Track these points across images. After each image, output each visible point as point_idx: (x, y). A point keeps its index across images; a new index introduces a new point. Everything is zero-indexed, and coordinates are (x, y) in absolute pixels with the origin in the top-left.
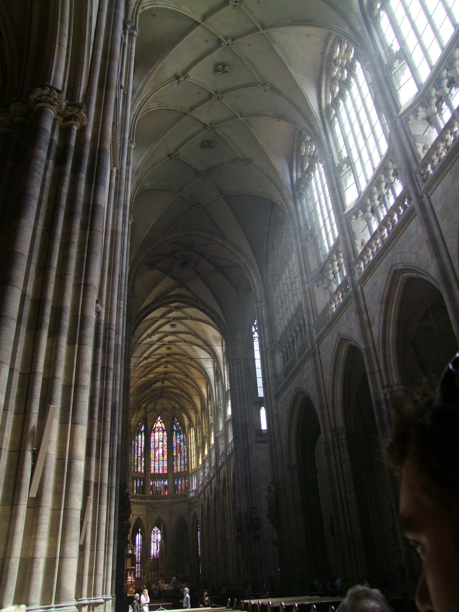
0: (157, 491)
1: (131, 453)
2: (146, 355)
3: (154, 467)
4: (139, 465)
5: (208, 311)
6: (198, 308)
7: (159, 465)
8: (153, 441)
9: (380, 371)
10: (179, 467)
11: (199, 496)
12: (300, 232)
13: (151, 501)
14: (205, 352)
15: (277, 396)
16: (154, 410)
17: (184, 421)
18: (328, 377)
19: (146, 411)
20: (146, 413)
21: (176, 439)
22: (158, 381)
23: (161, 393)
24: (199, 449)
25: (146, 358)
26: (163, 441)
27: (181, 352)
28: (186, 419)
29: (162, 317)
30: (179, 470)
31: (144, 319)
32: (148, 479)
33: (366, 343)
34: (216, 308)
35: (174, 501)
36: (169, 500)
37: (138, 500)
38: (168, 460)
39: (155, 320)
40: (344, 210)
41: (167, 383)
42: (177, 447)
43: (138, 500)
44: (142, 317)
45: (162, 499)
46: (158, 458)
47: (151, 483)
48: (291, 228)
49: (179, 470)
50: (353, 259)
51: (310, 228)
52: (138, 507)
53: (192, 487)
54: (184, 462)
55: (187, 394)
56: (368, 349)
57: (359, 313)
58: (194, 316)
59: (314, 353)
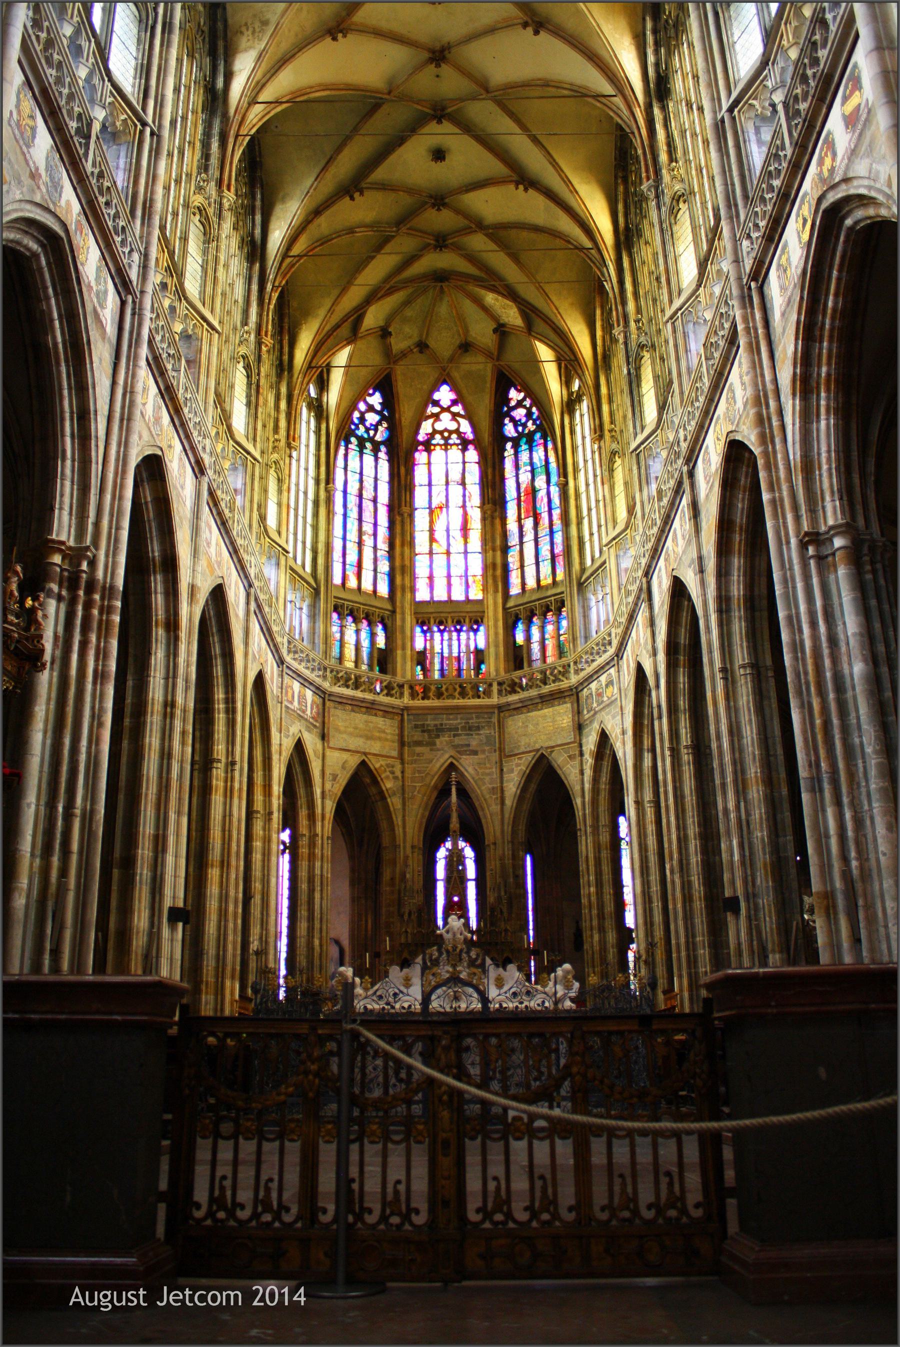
0: (442, 670)
1: (330, 513)
3: (431, 578)
4: (368, 564)
7: (450, 566)
10: (530, 572)
13: (419, 703)
16: (422, 346)
21: (517, 467)
24: (611, 461)
26: (463, 483)
30: (531, 583)
32: (403, 620)
35: (513, 698)
36: (495, 700)
37: (359, 694)
38: (484, 551)
42: (519, 498)
43: (359, 694)
45: (463, 694)
47: (419, 644)
49: (531, 583)
52: (360, 719)
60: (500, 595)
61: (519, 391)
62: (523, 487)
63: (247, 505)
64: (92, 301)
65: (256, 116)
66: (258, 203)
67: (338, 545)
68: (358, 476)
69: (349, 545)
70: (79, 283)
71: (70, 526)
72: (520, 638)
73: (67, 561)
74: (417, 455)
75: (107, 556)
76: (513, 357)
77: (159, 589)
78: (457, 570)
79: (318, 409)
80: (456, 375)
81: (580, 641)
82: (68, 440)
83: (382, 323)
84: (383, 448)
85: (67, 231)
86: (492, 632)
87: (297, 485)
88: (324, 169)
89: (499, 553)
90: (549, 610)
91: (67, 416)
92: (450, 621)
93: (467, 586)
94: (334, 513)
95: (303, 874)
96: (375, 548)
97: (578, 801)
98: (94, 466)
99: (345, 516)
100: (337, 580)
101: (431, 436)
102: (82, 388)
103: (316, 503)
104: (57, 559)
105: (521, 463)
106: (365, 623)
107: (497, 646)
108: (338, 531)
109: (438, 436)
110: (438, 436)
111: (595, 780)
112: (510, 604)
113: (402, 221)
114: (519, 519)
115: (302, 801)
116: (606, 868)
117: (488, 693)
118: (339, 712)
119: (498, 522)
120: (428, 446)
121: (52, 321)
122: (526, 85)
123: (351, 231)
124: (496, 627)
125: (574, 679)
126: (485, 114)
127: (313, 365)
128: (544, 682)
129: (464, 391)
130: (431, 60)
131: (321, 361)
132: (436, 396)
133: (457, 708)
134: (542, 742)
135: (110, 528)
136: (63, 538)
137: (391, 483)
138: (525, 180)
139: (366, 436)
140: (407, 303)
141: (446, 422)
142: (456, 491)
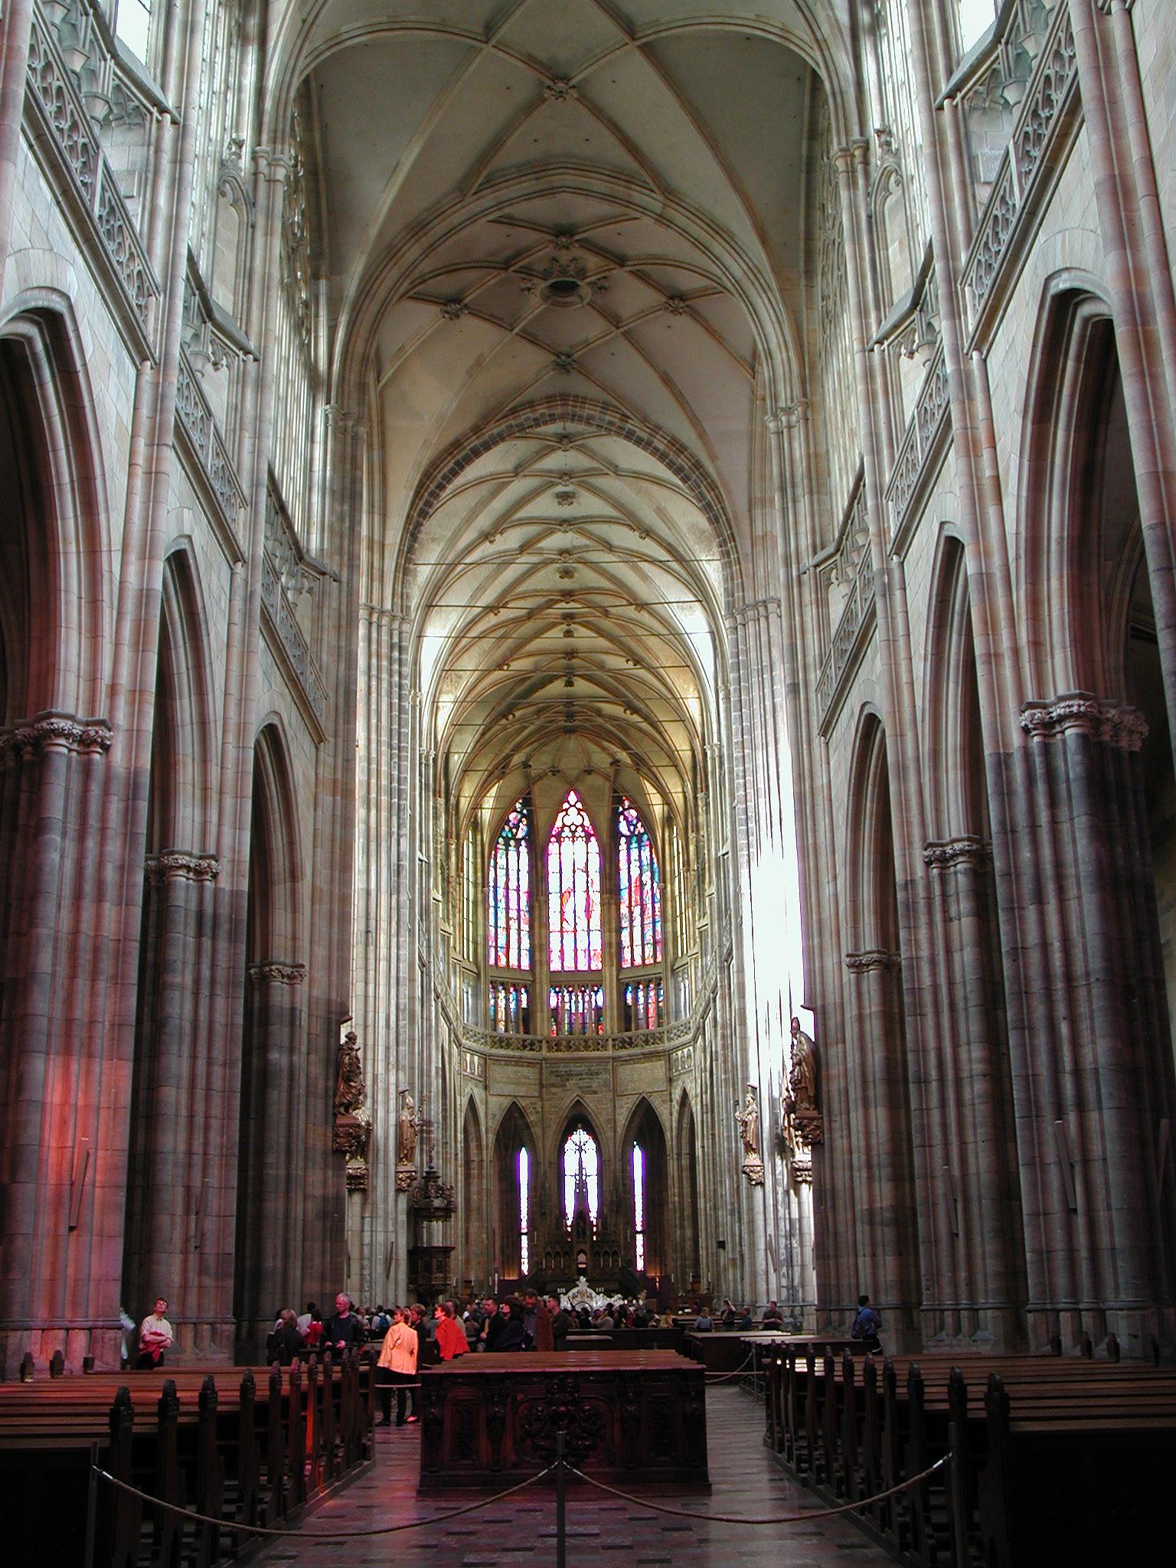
0: (570, 1023)
2: (487, 599)
3: (562, 951)
5: (661, 447)
6: (629, 436)
9: (1016, 651)
10: (638, 951)
11: (695, 1039)
12: (866, 162)
14: (679, 584)
15: (826, 728)
16: (555, 771)
17: (649, 805)
18: (921, 669)
19: (527, 777)
20: (530, 781)
21: (629, 862)
22: (551, 679)
23: (570, 716)
25: (492, 609)
26: (587, 872)
27: (607, 584)
28: (655, 799)
29: (518, 471)
30: (638, 961)
31: (449, 481)
33: (983, 554)
34: (687, 435)
35: (623, 1053)
36: (610, 1053)
37: (510, 1052)
39: (498, 482)
40: (950, 73)
41: (582, 686)
43: (510, 1052)
44: (445, 477)
45: (587, 1048)
47: (553, 1002)
48: (835, 147)
49: (638, 961)
50: (963, 257)
51: (894, 146)
53: (677, 1012)
54: (654, 937)
55: (646, 719)
56: (988, 575)
57: (971, 451)
58: (624, 464)
59: (891, 586)
72: (629, 1001)
76: (628, 778)
78: (582, 945)
80: (581, 788)
81: (672, 1015)
90: (650, 981)
95: (474, 1188)
96: (519, 930)
97: (668, 1135)
100: (492, 961)
103: (475, 903)
108: (492, 922)
111: (680, 1121)
114: (630, 906)
115: (472, 1136)
116: (686, 1184)
117: (605, 1048)
118: (496, 1068)
123: (505, 728)
125: (667, 1045)
128: (647, 1042)
129: (588, 801)
133: (582, 1059)
134: (644, 1088)
142: (581, 877)
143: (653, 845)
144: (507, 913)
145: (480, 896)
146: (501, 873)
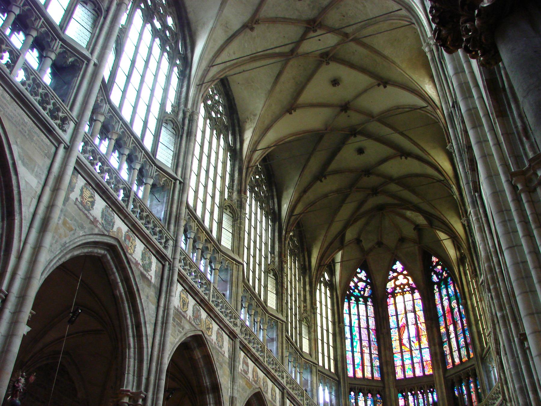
3: (403, 365)
4: (367, 363)
8: (394, 313)
10: (456, 354)
16: (380, 244)
19: (362, 250)
21: (441, 298)
23: (375, 191)
26: (414, 311)
30: (457, 361)
32: (390, 391)
38: (430, 347)
42: (444, 315)
46: (408, 345)
49: (457, 361)
54: (465, 341)
60: (441, 370)
61: (437, 257)
62: (446, 308)
63: (280, 345)
64: (139, 269)
65: (257, 156)
66: (275, 193)
67: (349, 355)
68: (356, 317)
69: (355, 354)
70: (129, 263)
71: (133, 382)
73: (132, 400)
74: (388, 300)
75: (153, 394)
77: (212, 402)
79: (330, 285)
82: (131, 339)
83: (356, 236)
84: (369, 300)
85: (119, 242)
86: (439, 392)
87: (322, 327)
88: (302, 171)
89: (437, 346)
91: (130, 327)
92: (416, 389)
93: (423, 367)
94: (346, 338)
96: (371, 354)
98: (145, 350)
99: (352, 339)
100: (350, 374)
101: (394, 289)
102: (136, 312)
103: (334, 335)
104: (126, 400)
105: (443, 295)
106: (369, 395)
107: (443, 399)
109: (398, 288)
110: (398, 288)
112: (447, 375)
113: (352, 186)
119: (435, 330)
120: (393, 294)
121: (117, 283)
122: (389, 110)
123: (326, 196)
124: (441, 389)
126: (375, 127)
127: (322, 264)
130: (342, 111)
131: (328, 261)
132: (394, 267)
135: (155, 380)
136: (129, 388)
137: (375, 318)
138: (405, 154)
139: (359, 295)
140: (367, 224)
141: (401, 280)
142: (411, 316)
143: (454, 282)
144: (361, 344)
145: (337, 329)
146: (354, 318)
